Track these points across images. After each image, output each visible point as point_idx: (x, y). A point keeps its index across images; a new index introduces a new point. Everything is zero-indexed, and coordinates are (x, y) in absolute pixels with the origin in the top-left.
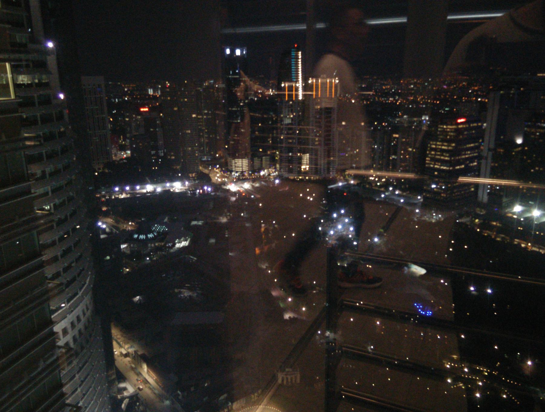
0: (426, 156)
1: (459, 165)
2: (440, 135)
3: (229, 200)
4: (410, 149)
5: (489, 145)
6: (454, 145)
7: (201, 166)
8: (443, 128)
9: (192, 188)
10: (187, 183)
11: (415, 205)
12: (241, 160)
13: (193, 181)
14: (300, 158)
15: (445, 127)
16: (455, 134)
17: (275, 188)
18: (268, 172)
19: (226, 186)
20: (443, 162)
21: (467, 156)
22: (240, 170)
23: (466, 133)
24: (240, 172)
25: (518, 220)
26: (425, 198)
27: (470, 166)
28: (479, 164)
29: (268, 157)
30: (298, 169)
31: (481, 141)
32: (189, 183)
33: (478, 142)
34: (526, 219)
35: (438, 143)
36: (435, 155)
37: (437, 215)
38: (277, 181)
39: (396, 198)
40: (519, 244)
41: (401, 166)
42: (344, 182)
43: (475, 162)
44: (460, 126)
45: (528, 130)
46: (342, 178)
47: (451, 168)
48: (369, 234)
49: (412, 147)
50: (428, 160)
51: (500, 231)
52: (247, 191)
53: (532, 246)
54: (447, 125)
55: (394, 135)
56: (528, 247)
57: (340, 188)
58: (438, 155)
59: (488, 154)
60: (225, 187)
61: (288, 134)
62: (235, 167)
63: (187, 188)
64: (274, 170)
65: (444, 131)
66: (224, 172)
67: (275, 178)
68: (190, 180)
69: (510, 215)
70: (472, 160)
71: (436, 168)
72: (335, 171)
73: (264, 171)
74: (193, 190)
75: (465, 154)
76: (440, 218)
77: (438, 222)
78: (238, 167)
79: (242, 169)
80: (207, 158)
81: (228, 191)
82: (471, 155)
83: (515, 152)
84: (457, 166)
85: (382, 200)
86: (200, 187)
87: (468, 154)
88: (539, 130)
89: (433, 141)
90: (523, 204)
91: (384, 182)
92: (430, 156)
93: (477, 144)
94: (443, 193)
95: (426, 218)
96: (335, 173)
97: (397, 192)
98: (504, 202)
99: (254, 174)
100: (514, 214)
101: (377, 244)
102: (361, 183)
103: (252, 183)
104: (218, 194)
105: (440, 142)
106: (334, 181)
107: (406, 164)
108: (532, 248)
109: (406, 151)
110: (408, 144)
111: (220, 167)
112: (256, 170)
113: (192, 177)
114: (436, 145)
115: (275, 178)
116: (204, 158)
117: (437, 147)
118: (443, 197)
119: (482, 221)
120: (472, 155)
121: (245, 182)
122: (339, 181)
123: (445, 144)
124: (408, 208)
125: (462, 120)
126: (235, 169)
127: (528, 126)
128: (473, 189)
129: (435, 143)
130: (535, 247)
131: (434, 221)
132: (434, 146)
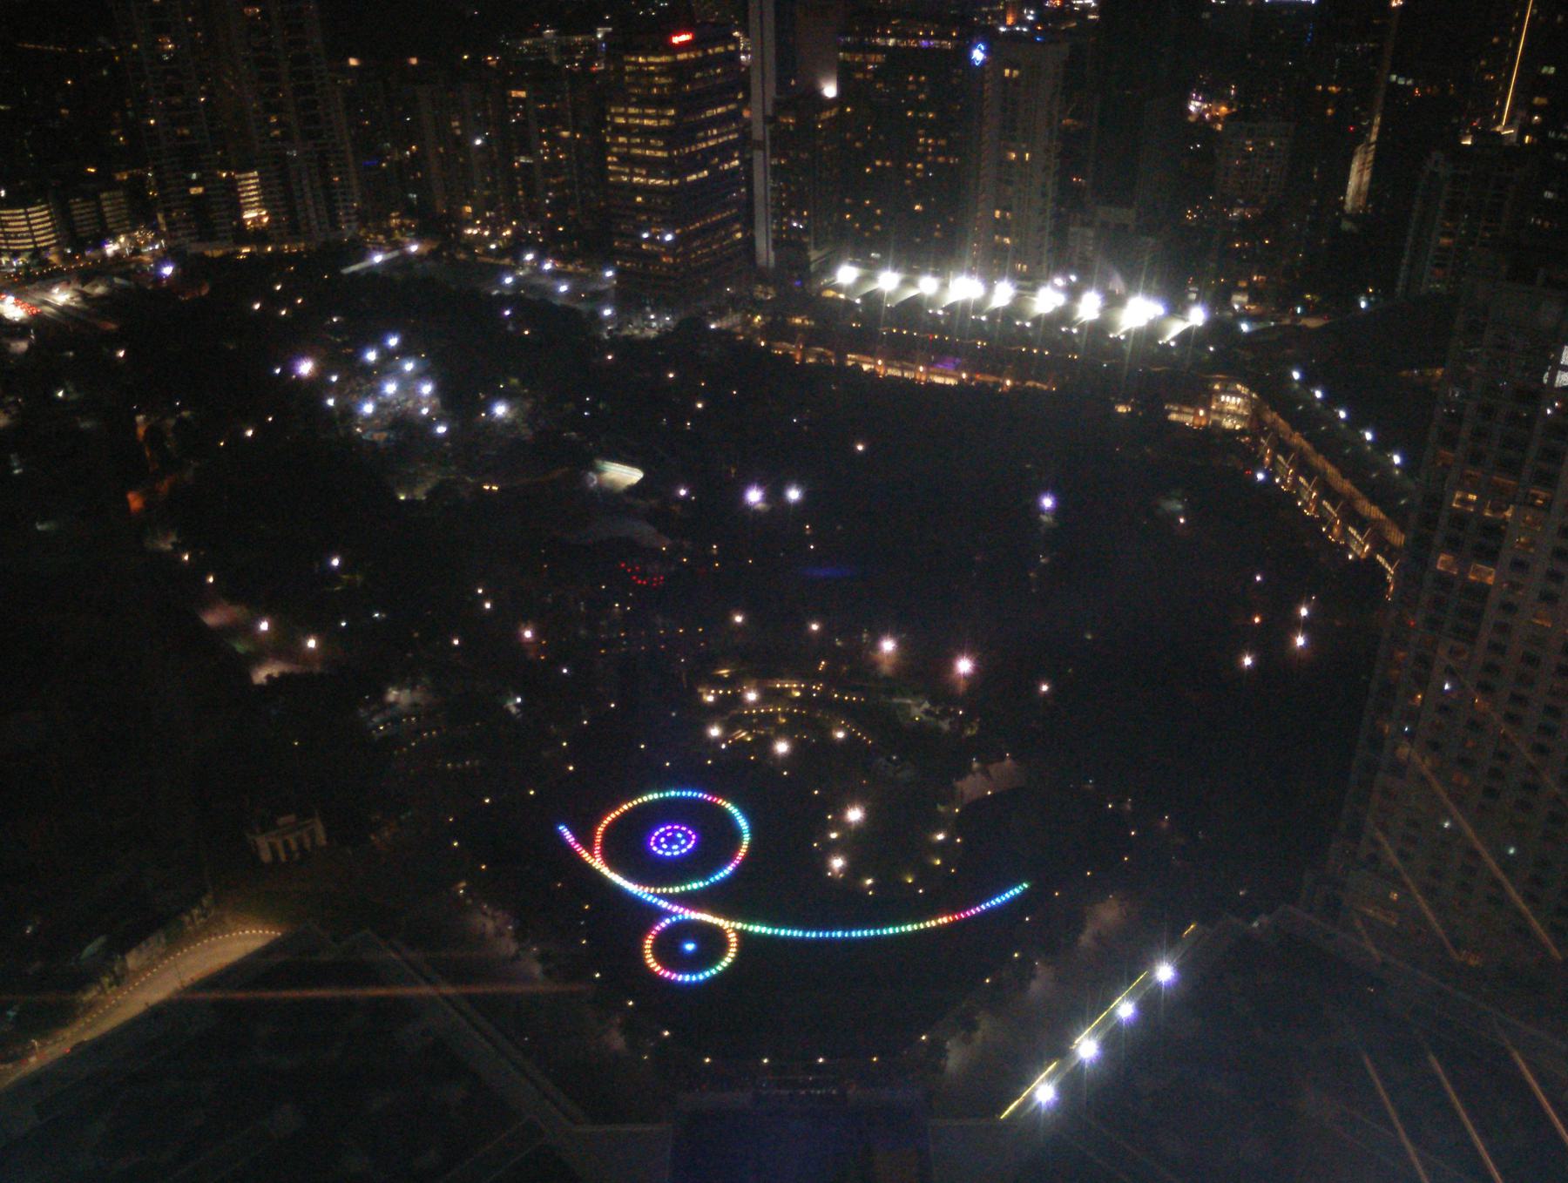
0: (604, 150)
1: (695, 172)
4: (565, 134)
5: (764, 109)
6: (672, 112)
8: (636, 63)
11: (599, 298)
12: (21, 211)
14: (231, 185)
15: (641, 60)
16: (670, 80)
18: (131, 244)
20: (653, 167)
21: (711, 143)
23: (698, 75)
24: (27, 254)
25: (849, 304)
26: (620, 273)
28: (747, 163)
30: (231, 224)
31: (740, 96)
33: (735, 100)
34: (866, 297)
35: (632, 110)
36: (630, 145)
38: (168, 270)
39: (542, 281)
40: (857, 367)
41: (548, 189)
43: (733, 159)
44: (682, 57)
45: (848, 57)
47: (675, 182)
48: (482, 396)
50: (613, 163)
51: (811, 338)
53: (887, 365)
54: (645, 56)
55: (514, 94)
56: (878, 370)
58: (637, 146)
59: (764, 129)
62: (7, 236)
64: (150, 236)
65: (640, 71)
67: (161, 260)
69: (830, 293)
70: (724, 152)
71: (638, 184)
72: (354, 217)
73: (115, 240)
75: (706, 139)
76: (666, 326)
77: (665, 336)
78: (16, 238)
79: (35, 243)
82: (720, 141)
83: (822, 122)
84: (691, 173)
85: (508, 293)
87: (713, 137)
88: (872, 57)
89: (616, 105)
90: (859, 260)
92: (615, 149)
93: (732, 107)
94: (665, 255)
95: (633, 330)
97: (548, 266)
98: (815, 261)
99: (83, 257)
100: (838, 289)
101: (506, 421)
103: (79, 287)
105: (635, 105)
107: (561, 179)
108: (886, 371)
109: (554, 139)
110: (552, 119)
114: (626, 116)
115: (161, 260)
117: (631, 121)
118: (667, 265)
119: (769, 319)
120: (725, 138)
121: (54, 284)
122: (374, 249)
123: (650, 111)
124: (581, 307)
125: (685, 38)
126: (7, 244)
127: (846, 48)
128: (739, 235)
130: (891, 366)
131: (652, 334)
132: (621, 121)
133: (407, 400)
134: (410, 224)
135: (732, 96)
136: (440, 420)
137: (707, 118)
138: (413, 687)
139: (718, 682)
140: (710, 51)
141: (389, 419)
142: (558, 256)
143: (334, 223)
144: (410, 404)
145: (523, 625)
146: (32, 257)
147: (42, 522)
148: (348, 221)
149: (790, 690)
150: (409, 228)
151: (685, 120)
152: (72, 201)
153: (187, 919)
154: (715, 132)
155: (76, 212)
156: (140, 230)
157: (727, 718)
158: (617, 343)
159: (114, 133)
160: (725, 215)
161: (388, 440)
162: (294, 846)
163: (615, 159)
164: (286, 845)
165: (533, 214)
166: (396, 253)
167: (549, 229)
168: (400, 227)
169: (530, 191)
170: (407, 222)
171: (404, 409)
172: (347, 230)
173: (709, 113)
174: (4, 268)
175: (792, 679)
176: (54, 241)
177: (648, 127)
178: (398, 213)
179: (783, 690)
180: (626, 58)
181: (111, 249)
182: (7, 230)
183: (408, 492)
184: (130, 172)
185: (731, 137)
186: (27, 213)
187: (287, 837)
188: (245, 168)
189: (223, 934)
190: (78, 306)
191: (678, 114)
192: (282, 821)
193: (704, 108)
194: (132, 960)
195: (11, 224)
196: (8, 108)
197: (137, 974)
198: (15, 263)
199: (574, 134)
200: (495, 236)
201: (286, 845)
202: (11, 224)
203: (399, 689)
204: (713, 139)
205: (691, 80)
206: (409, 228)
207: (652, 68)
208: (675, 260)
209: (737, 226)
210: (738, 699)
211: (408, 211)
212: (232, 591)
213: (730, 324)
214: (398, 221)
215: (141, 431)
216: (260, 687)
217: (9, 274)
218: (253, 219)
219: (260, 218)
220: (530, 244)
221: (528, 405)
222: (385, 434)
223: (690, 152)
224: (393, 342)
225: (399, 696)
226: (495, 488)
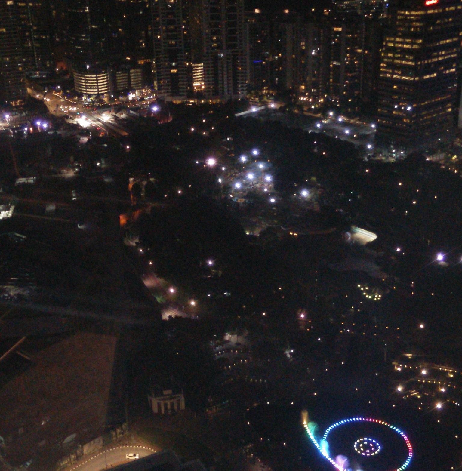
1: (430, 74)
2: (399, 26)
3: (78, 142)
4: (360, 51)
6: (421, 41)
7: (30, 88)
9: (15, 125)
10: (7, 116)
11: (365, 138)
12: (95, 76)
13: (17, 113)
14: (190, 70)
15: (407, 13)
16: (422, 24)
17: (152, 119)
18: (140, 95)
19: (73, 120)
20: (405, 70)
21: (440, 59)
22: (94, 91)
24: (94, 96)
26: (378, 125)
27: (446, 74)
29: (139, 70)
30: (187, 88)
32: (11, 117)
35: (398, 40)
36: (394, 58)
37: (397, 151)
38: (155, 109)
39: (336, 127)
42: (260, 106)
43: (453, 68)
44: (430, 12)
46: (257, 99)
47: (417, 79)
48: (296, 185)
49: (363, 48)
50: (383, 67)
52: (106, 125)
54: (409, 11)
57: (254, 116)
58: (398, 58)
60: (71, 121)
61: (167, 30)
63: (7, 124)
65: (406, 19)
66: (70, 96)
67: (152, 104)
68: (13, 111)
70: (447, 64)
71: (396, 79)
72: (245, 89)
73: (134, 92)
74: (17, 129)
75: (438, 56)
76: (401, 157)
77: (399, 163)
78: (91, 88)
79: (98, 91)
80: (40, 74)
81: (77, 126)
82: (446, 57)
84: (426, 75)
85: (317, 132)
86: (29, 122)
87: (442, 55)
89: (390, 36)
91: (322, 104)
92: (385, 60)
93: (455, 39)
95: (382, 157)
96: (245, 93)
97: (340, 120)
102: (285, 107)
103: (114, 114)
104: (59, 132)
105: (400, 37)
106: (245, 105)
107: (354, 74)
109: (353, 53)
110: (354, 43)
111: (64, 89)
112: (121, 91)
113: (16, 107)
114: (394, 42)
116: (36, 74)
117: (397, 45)
118: (406, 123)
120: (449, 56)
122: (253, 105)
123: (408, 40)
124: (356, 143)
128: (450, 110)
129: (392, 39)
131: (392, 160)
132: (391, 45)
133: (257, 183)
134: (273, 93)
135: (456, 33)
136: (273, 195)
137: (440, 45)
138: (239, 334)
139: (405, 361)
140: (447, 9)
141: (247, 192)
142: (346, 114)
143: (235, 91)
144: (258, 185)
145: (300, 310)
146: (96, 98)
147: (80, 225)
148: (242, 90)
149: (447, 372)
150: (271, 95)
151: (427, 46)
152: (118, 73)
153: (114, 433)
154: (443, 53)
155: (119, 78)
156: (145, 88)
157: (407, 382)
158: (371, 164)
159: (141, 41)
160: (443, 98)
161: (244, 203)
162: (169, 407)
163: (385, 65)
164: (166, 405)
165: (337, 91)
166: (263, 108)
167: (344, 101)
168: (267, 95)
169: (336, 80)
170: (271, 92)
171: (255, 188)
172: (242, 94)
173: (441, 42)
174: (83, 102)
175: (450, 365)
176: (107, 91)
177: (405, 48)
178: (267, 88)
179: (443, 371)
180: (399, 12)
181: (131, 97)
182: (87, 84)
183: (251, 231)
184: (145, 60)
185: (452, 56)
186: (97, 77)
187: (167, 401)
188: (197, 61)
189: (129, 445)
190: (112, 122)
191: (424, 41)
192: (166, 392)
193: (438, 41)
194: (86, 449)
195: (89, 82)
196: (97, 27)
197: (87, 457)
198: (88, 100)
199: (364, 51)
200: (315, 102)
201: (166, 405)
202: (89, 82)
203: (232, 334)
204: (442, 56)
205: (433, 24)
206: (271, 95)
207: (412, 17)
208: (411, 121)
209: (449, 105)
210: (417, 373)
211: (272, 86)
212: (160, 272)
213: (438, 158)
214: (267, 91)
215: (131, 186)
216: (165, 321)
217: (85, 105)
218: (197, 87)
219: (201, 86)
220: (333, 107)
221: (319, 192)
222: (244, 200)
223: (428, 63)
224: (255, 153)
225: (231, 337)
226: (295, 234)
